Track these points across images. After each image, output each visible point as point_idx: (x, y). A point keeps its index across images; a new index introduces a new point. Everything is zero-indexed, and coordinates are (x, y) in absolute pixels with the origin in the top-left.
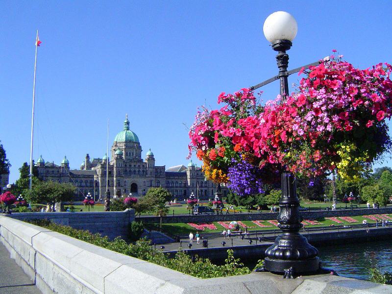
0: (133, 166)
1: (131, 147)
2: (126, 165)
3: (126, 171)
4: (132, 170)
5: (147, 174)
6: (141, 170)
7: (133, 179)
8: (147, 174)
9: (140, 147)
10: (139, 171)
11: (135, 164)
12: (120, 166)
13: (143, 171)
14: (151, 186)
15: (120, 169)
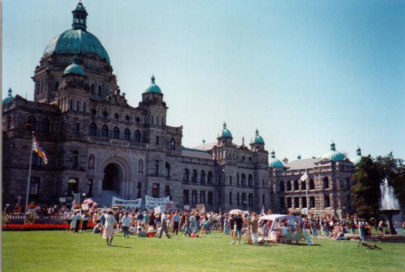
0: (112, 116)
1: (98, 72)
2: (94, 112)
3: (93, 127)
4: (111, 126)
5: (147, 141)
6: (133, 129)
7: (113, 152)
8: (147, 141)
9: (114, 77)
10: (128, 132)
11: (117, 110)
12: (82, 110)
13: (138, 134)
14: (157, 175)
15: (81, 117)
